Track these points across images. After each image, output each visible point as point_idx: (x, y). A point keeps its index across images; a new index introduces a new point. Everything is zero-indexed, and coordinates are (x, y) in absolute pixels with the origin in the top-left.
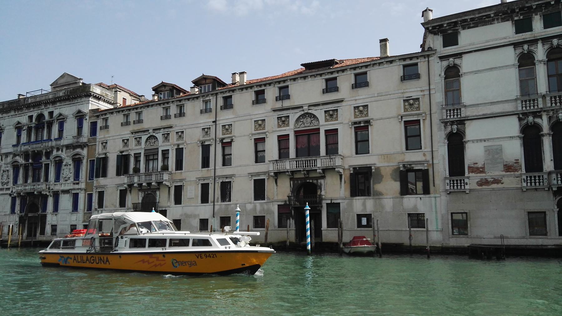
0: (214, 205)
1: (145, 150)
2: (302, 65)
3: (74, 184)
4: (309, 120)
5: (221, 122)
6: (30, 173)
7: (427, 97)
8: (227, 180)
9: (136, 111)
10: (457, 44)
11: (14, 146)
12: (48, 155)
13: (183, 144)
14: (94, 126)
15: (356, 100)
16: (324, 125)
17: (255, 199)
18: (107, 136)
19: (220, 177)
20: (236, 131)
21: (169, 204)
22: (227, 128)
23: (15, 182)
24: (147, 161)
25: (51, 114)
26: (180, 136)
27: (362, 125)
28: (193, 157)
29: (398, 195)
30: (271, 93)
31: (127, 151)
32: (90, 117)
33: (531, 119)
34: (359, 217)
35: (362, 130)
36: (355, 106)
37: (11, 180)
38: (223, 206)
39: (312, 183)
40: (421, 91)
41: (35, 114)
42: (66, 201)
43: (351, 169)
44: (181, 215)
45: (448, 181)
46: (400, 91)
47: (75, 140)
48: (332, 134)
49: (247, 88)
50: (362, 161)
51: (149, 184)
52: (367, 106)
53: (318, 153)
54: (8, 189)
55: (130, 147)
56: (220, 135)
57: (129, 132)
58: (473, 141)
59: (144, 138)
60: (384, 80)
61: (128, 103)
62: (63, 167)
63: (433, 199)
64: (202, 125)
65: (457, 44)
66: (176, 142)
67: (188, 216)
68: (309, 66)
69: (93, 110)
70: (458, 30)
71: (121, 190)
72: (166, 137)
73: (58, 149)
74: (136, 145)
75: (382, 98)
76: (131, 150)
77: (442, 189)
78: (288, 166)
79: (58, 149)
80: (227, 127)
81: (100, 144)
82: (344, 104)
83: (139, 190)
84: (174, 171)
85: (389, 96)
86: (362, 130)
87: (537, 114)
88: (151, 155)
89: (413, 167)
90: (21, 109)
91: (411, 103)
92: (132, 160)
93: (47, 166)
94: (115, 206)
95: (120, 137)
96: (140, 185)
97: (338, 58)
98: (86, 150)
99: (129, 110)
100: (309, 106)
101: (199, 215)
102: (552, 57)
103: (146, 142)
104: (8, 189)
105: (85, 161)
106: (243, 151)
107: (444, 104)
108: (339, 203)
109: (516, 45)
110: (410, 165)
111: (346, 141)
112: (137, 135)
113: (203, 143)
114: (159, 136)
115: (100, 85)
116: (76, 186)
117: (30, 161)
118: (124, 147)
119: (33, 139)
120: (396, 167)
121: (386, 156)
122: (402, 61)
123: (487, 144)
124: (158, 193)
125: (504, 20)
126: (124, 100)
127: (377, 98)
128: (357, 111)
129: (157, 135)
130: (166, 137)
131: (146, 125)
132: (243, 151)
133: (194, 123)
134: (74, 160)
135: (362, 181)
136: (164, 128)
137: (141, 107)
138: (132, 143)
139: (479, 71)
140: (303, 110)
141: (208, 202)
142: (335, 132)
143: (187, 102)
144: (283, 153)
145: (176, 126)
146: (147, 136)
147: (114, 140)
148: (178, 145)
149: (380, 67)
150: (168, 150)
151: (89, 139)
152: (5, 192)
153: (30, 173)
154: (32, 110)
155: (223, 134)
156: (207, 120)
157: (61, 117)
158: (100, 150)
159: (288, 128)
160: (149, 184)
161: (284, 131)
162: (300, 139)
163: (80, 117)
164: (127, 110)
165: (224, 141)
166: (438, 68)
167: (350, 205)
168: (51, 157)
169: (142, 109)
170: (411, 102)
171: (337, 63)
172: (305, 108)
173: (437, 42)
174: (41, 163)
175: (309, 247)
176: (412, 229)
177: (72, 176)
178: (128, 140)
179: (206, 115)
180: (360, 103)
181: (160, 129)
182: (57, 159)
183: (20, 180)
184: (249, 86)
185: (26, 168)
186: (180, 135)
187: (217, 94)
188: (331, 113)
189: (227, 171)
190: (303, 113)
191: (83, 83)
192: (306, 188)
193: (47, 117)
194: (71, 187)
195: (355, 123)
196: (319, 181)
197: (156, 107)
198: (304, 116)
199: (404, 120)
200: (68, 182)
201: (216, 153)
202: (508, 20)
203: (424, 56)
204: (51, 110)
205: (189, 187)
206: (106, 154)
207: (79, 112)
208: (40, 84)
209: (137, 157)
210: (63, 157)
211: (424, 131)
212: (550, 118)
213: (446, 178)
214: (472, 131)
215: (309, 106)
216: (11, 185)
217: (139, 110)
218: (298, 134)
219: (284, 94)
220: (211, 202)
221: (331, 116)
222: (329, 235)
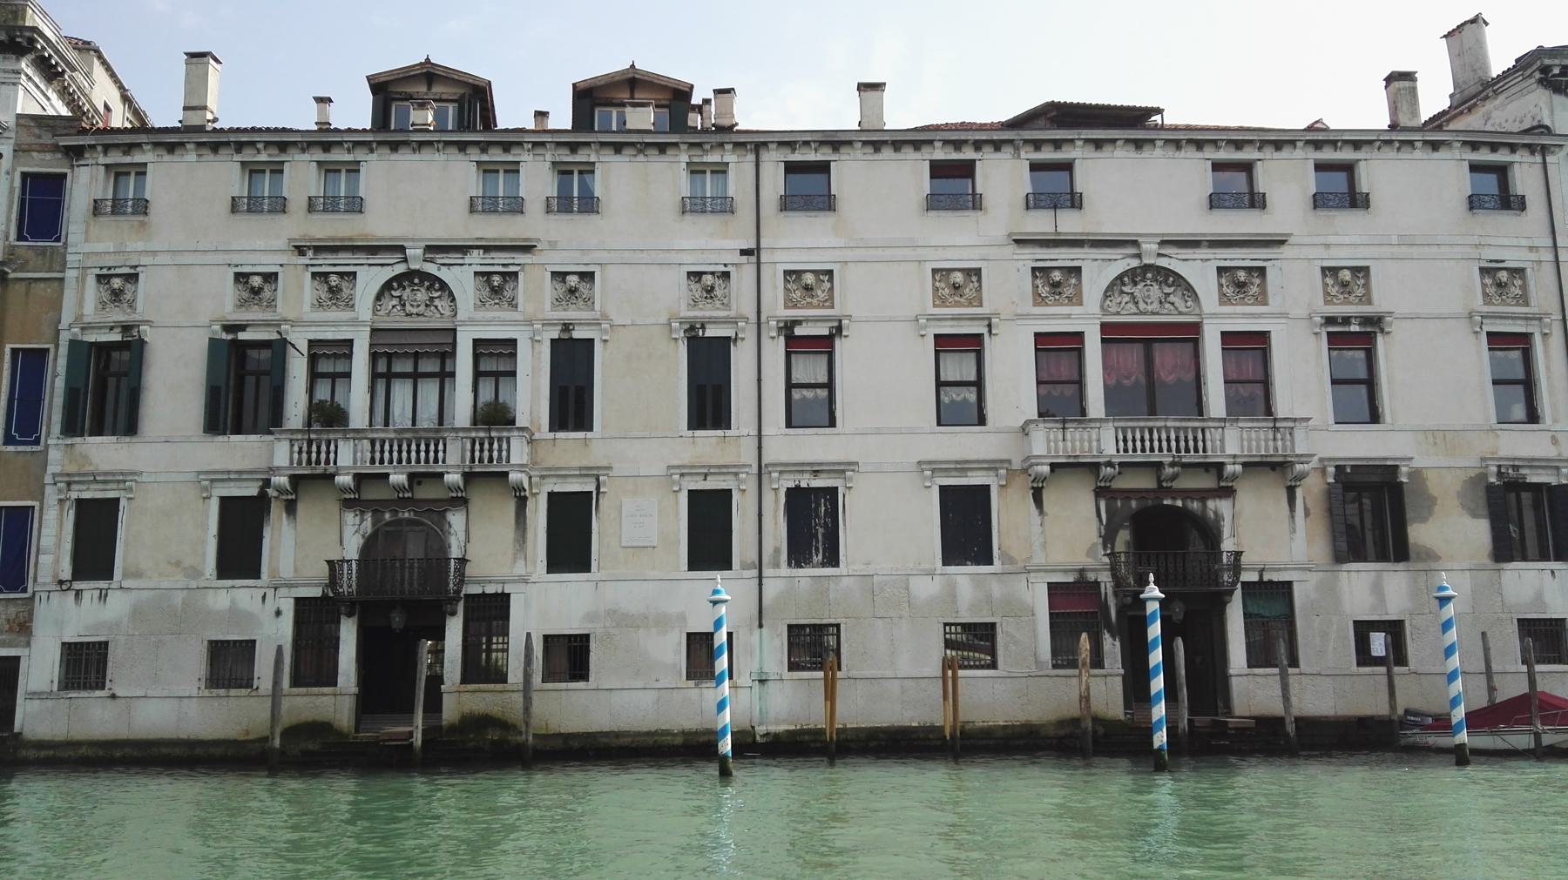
0: (760, 577)
1: (374, 331)
4: (1155, 291)
5: (778, 256)
7: (1549, 269)
9: (320, 156)
13: (596, 323)
15: (1327, 246)
16: (1219, 317)
17: (947, 561)
18: (140, 246)
19: (786, 468)
20: (852, 298)
21: (520, 569)
22: (808, 283)
24: (382, 377)
27: (1355, 328)
28: (641, 385)
29: (1487, 561)
30: (1003, 178)
31: (267, 324)
32: (18, 150)
34: (1363, 630)
36: (1326, 264)
38: (805, 584)
39: (1185, 507)
40: (1531, 248)
43: (1331, 470)
44: (591, 617)
46: (1470, 240)
48: (1250, 348)
49: (897, 145)
50: (1362, 445)
52: (1366, 270)
55: (284, 309)
56: (777, 307)
57: (281, 243)
59: (371, 278)
60: (1420, 197)
64: (687, 258)
69: (41, 121)
71: (224, 501)
72: (498, 286)
74: (320, 304)
75: (1415, 251)
76: (294, 323)
81: (91, 281)
82: (1285, 251)
83: (348, 504)
84: (543, 431)
85: (1434, 249)
88: (412, 356)
89: (1524, 477)
91: (1500, 279)
92: (298, 368)
94: (195, 573)
95: (221, 258)
99: (283, 147)
100: (1163, 243)
101: (682, 618)
103: (379, 297)
106: (886, 376)
108: (1290, 583)
111: (1301, 375)
112: (326, 263)
113: (692, 328)
114: (461, 277)
118: (242, 304)
120: (1472, 473)
121: (1436, 436)
122: (1468, 149)
124: (456, 519)
127: (1396, 250)
128: (1329, 281)
129: (444, 274)
130: (498, 286)
131: (376, 224)
132: (886, 376)
133: (642, 248)
135: (1372, 512)
136: (487, 249)
137: (356, 144)
140: (1139, 256)
141: (726, 564)
142: (1256, 343)
143: (608, 156)
144: (1059, 397)
145: (553, 246)
146: (387, 274)
147: (181, 269)
148: (567, 327)
149: (1401, 155)
150: (513, 342)
155: (790, 303)
156: (714, 242)
158: (90, 310)
159: (1076, 310)
161: (1059, 319)
164: (268, 144)
165: (798, 331)
167: (1330, 591)
169: (359, 155)
170: (1503, 276)
175: (1160, 738)
176: (1539, 668)
178: (271, 278)
179: (709, 223)
180: (1342, 257)
181: (463, 249)
184: (915, 140)
186: (575, 284)
188: (1242, 276)
189: (813, 446)
190: (1135, 263)
192: (1165, 530)
195: (1330, 320)
196: (1211, 504)
197: (439, 157)
198: (1134, 276)
199: (1487, 328)
203: (1531, 148)
205: (628, 505)
206: (126, 328)
211: (1548, 368)
215: (1163, 243)
217: (337, 155)
218: (1113, 334)
219: (1055, 188)
220: (744, 567)
221: (1241, 286)
222: (1252, 691)
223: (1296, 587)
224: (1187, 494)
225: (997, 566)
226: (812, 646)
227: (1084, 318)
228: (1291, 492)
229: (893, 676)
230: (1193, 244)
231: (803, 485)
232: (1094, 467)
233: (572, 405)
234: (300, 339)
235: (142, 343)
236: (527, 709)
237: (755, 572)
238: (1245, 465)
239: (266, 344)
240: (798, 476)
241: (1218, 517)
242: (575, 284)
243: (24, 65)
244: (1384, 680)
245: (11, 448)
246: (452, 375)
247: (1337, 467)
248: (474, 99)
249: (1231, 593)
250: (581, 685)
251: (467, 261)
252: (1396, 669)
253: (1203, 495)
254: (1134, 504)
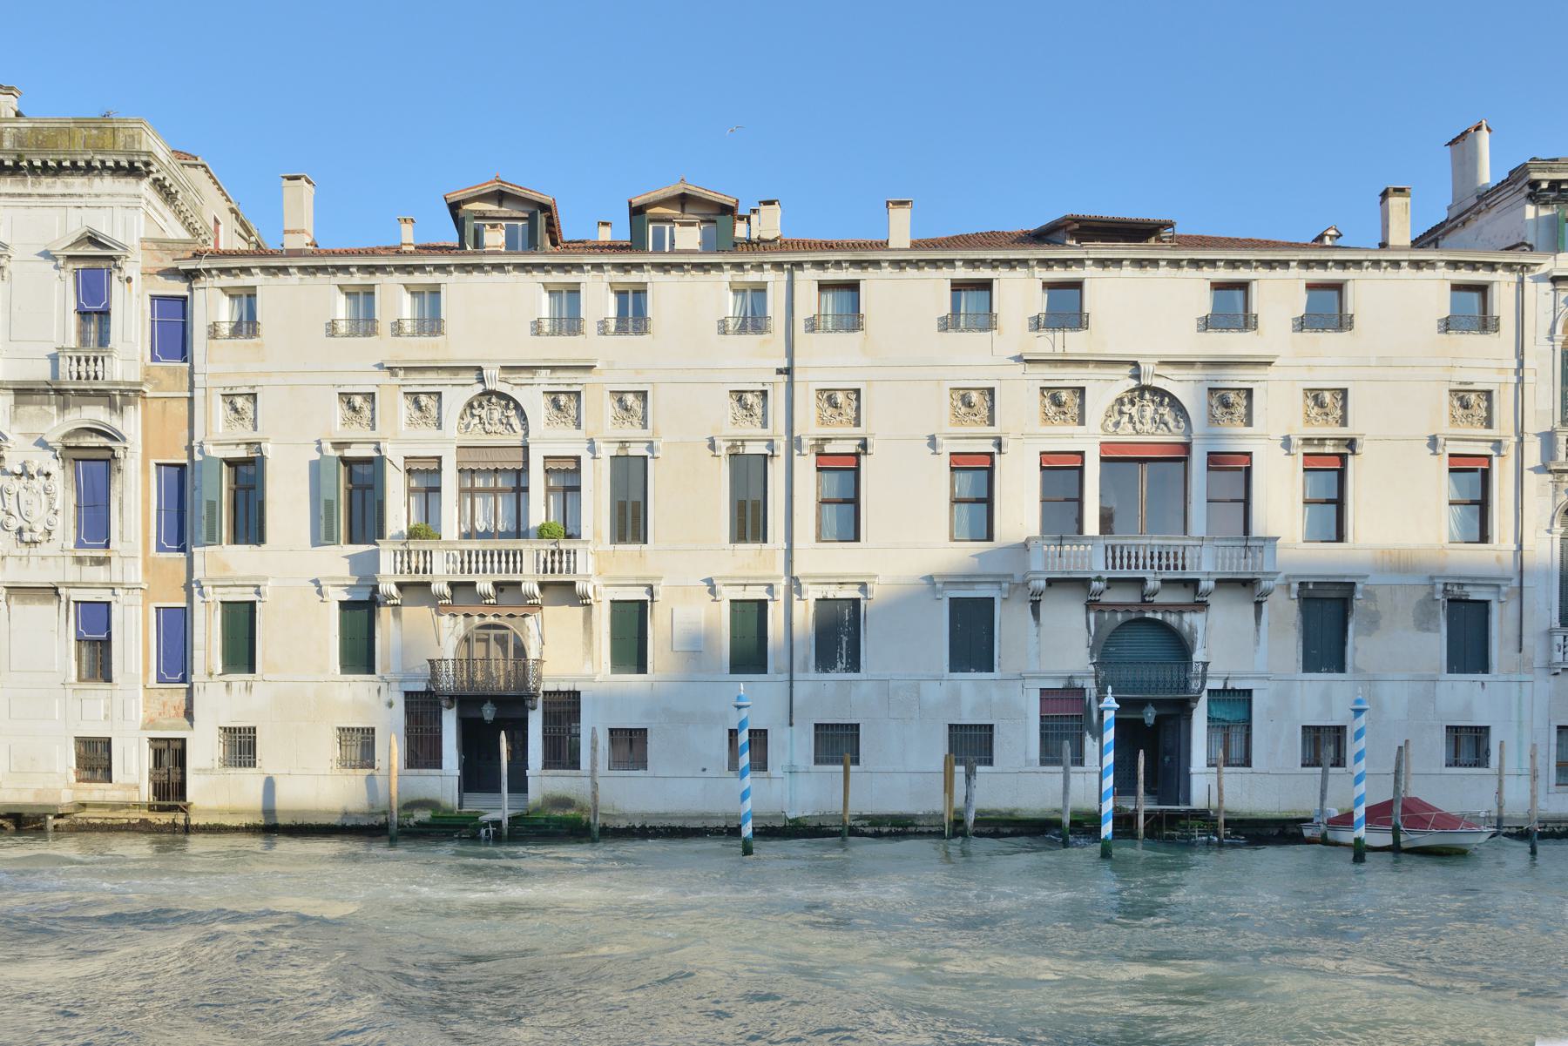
28: (690, 498)
35: (1330, 471)
43: (1295, 586)
77: (1539, 660)
78: (1089, 558)
86: (1330, 471)
110: (1461, 585)
134: (72, 454)
138: (395, 411)
151: (148, 376)
194: (72, 573)
196: (1187, 617)
201: (799, 490)
209: (426, 479)
213: (1550, 633)
223: (1255, 695)
224: (1167, 608)
225: (996, 674)
226: (838, 743)
227: (1088, 440)
228: (1258, 604)
229: (903, 771)
231: (830, 596)
232: (1084, 583)
233: (630, 521)
234: (395, 454)
235: (263, 458)
236: (594, 796)
237: (786, 676)
238: (1218, 581)
239: (368, 461)
240: (826, 587)
241: (1193, 630)
244: (1319, 778)
245: (163, 555)
246: (526, 489)
247: (1301, 584)
249: (1196, 700)
250: (641, 772)
251: (536, 381)
253: (1180, 609)
254: (1119, 616)
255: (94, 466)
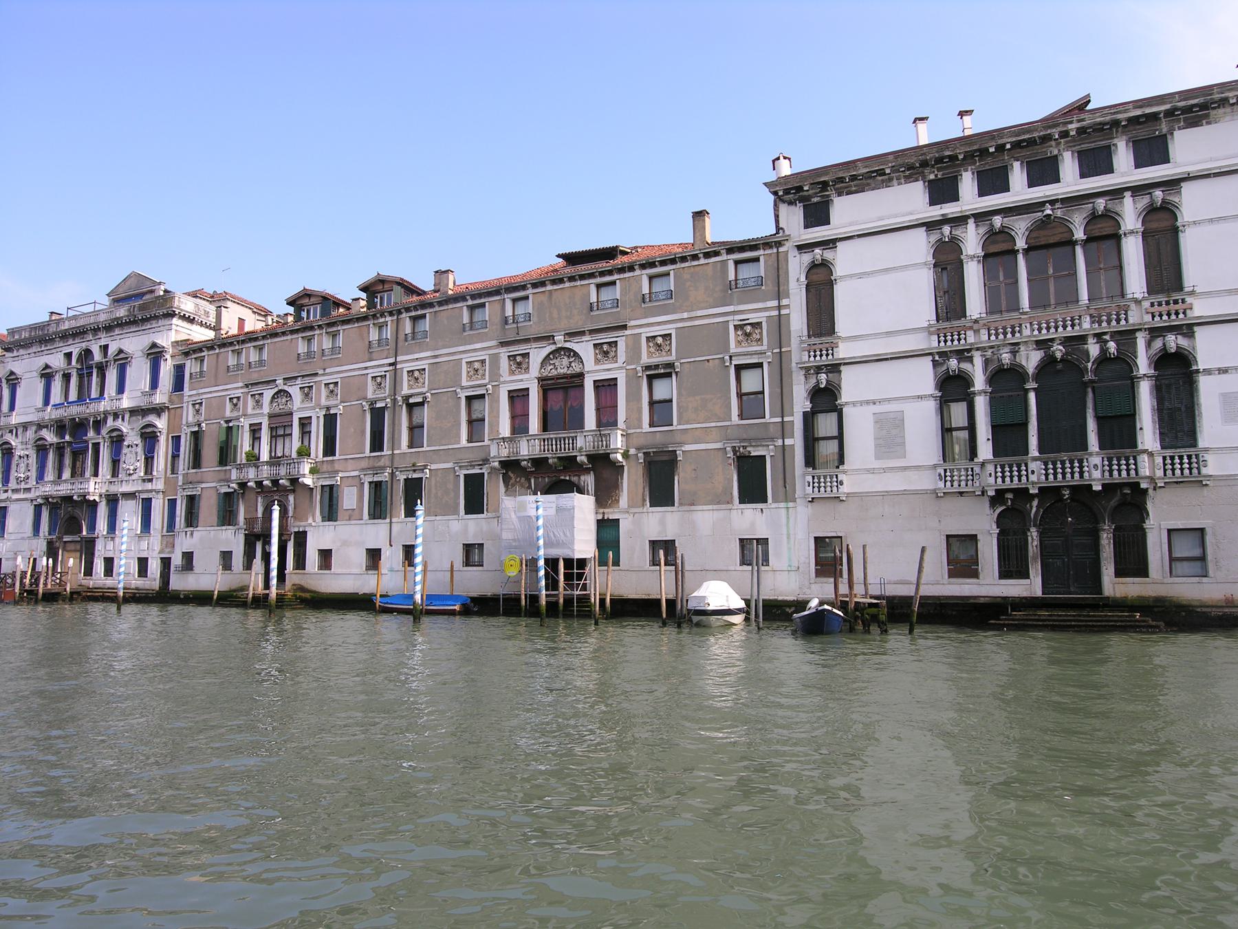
2: (558, 256)
3: (144, 481)
4: (565, 361)
6: (68, 461)
8: (415, 476)
10: (827, 222)
11: (38, 410)
12: (98, 425)
14: (179, 370)
16: (593, 370)
23: (40, 476)
24: (274, 437)
25: (105, 348)
26: (332, 392)
33: (953, 363)
37: (33, 474)
41: (75, 351)
42: (129, 516)
43: (640, 455)
45: (810, 479)
47: (146, 399)
51: (275, 482)
53: (579, 424)
54: (29, 490)
58: (854, 404)
59: (268, 394)
61: (248, 328)
62: (125, 450)
63: (783, 512)
65: (827, 222)
66: (324, 402)
67: (345, 543)
68: (572, 259)
70: (828, 196)
72: (307, 392)
73: (116, 416)
79: (116, 416)
80: (416, 374)
87: (964, 355)
90: (52, 340)
93: (96, 446)
96: (259, 484)
97: (625, 243)
98: (165, 416)
102: (993, 249)
103: (272, 402)
104: (29, 490)
105: (162, 439)
107: (805, 333)
109: (930, 226)
112: (255, 390)
114: (295, 391)
115: (194, 295)
116: (149, 486)
117: (67, 438)
119: (73, 396)
123: (877, 408)
125: (909, 179)
126: (241, 321)
129: (289, 390)
134: (144, 436)
139: (864, 273)
148: (328, 409)
152: (21, 496)
153: (68, 461)
154: (71, 342)
155: (410, 387)
157: (122, 356)
158: (191, 419)
160: (275, 482)
162: (552, 396)
163: (155, 355)
165: (411, 401)
166: (797, 266)
168: (104, 431)
170: (748, 329)
171: (624, 253)
172: (559, 338)
173: (793, 217)
174: (86, 442)
177: (141, 465)
178: (238, 398)
181: (296, 378)
182: (114, 434)
183: (50, 475)
185: (60, 449)
187: (399, 312)
190: (553, 347)
191: (166, 291)
193: (97, 357)
195: (648, 368)
196: (582, 478)
199: (734, 363)
200: (134, 477)
202: (917, 180)
204: (103, 343)
207: (154, 345)
208: (83, 293)
210: (125, 430)
212: (987, 362)
214: (852, 386)
216: (32, 482)
221: (606, 353)
230: (582, 333)
242: (332, 388)
243: (175, 321)
248: (329, 302)
252: (763, 568)
255: (149, 438)
